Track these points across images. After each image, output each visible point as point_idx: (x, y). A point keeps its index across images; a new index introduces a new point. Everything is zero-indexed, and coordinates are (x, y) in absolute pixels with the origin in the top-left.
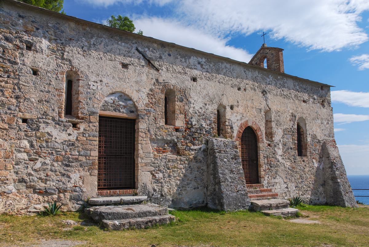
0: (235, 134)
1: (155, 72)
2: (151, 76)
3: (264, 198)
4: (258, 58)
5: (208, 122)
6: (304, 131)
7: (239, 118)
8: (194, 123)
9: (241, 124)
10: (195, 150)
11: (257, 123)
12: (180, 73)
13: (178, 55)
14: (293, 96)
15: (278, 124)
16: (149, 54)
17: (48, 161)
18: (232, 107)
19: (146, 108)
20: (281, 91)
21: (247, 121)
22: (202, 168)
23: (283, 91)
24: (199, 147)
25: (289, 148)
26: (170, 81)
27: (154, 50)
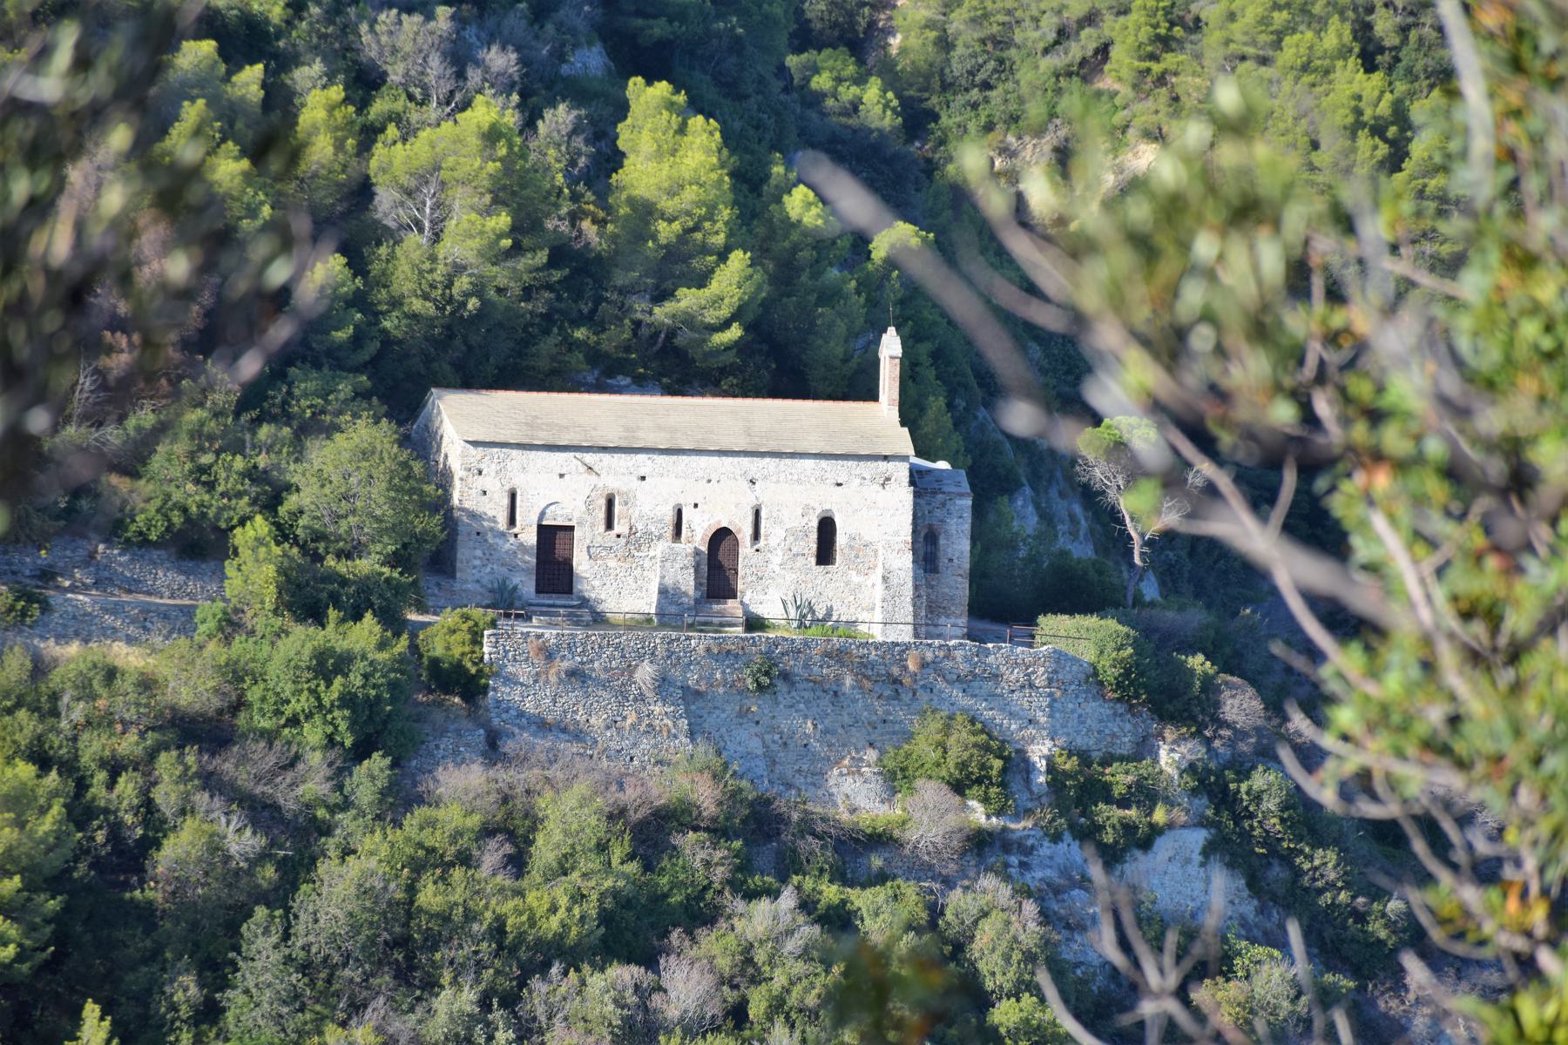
1: (594, 477)
5: (660, 526)
14: (813, 480)
15: (778, 521)
17: (495, 567)
18: (696, 506)
21: (719, 522)
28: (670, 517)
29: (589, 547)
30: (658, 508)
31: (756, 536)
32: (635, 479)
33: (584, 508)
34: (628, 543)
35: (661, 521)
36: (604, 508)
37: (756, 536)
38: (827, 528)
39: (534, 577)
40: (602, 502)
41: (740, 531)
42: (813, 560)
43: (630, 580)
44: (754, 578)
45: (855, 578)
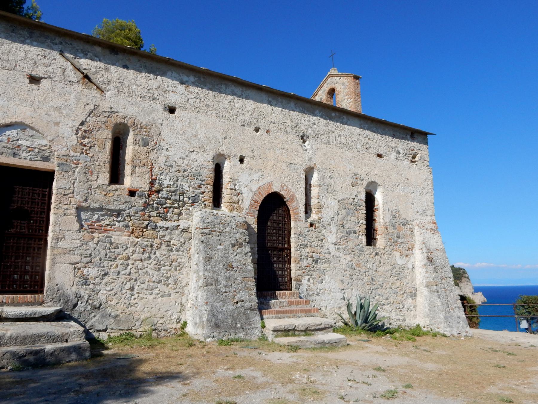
0: (246, 204)
1: (95, 93)
2: (84, 100)
3: (291, 315)
4: (324, 91)
6: (380, 204)
7: (256, 176)
8: (166, 183)
9: (259, 188)
10: (167, 229)
11: (290, 187)
12: (143, 97)
13: (141, 67)
14: (359, 146)
15: (330, 190)
18: (242, 160)
19: (72, 153)
20: (337, 136)
21: (270, 184)
22: (179, 260)
23: (340, 136)
24: (175, 224)
25: (350, 231)
26: (121, 110)
27: (96, 57)
28: (208, 173)
29: (79, 209)
30: (193, 156)
32: (160, 108)
34: (146, 205)
35: (196, 176)
36: (108, 146)
40: (107, 135)
41: (293, 198)
43: (150, 265)
44: (310, 261)
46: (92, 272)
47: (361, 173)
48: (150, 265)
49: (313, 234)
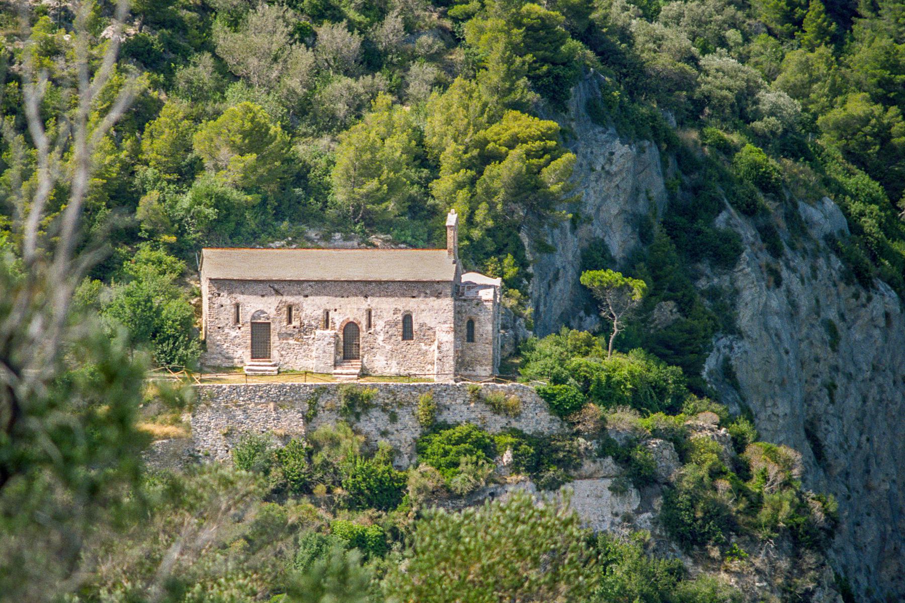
0: (337, 326)
16: (276, 287)
31: (369, 326)
33: (275, 313)
34: (299, 331)
37: (369, 326)
38: (407, 319)
39: (249, 350)
42: (400, 338)
45: (423, 347)
46: (283, 353)
47: (399, 307)
48: (301, 351)
49: (371, 339)
